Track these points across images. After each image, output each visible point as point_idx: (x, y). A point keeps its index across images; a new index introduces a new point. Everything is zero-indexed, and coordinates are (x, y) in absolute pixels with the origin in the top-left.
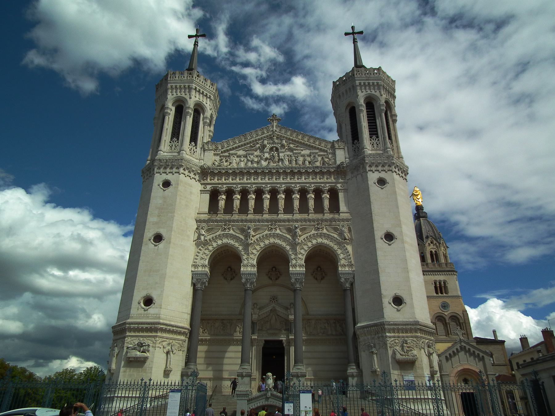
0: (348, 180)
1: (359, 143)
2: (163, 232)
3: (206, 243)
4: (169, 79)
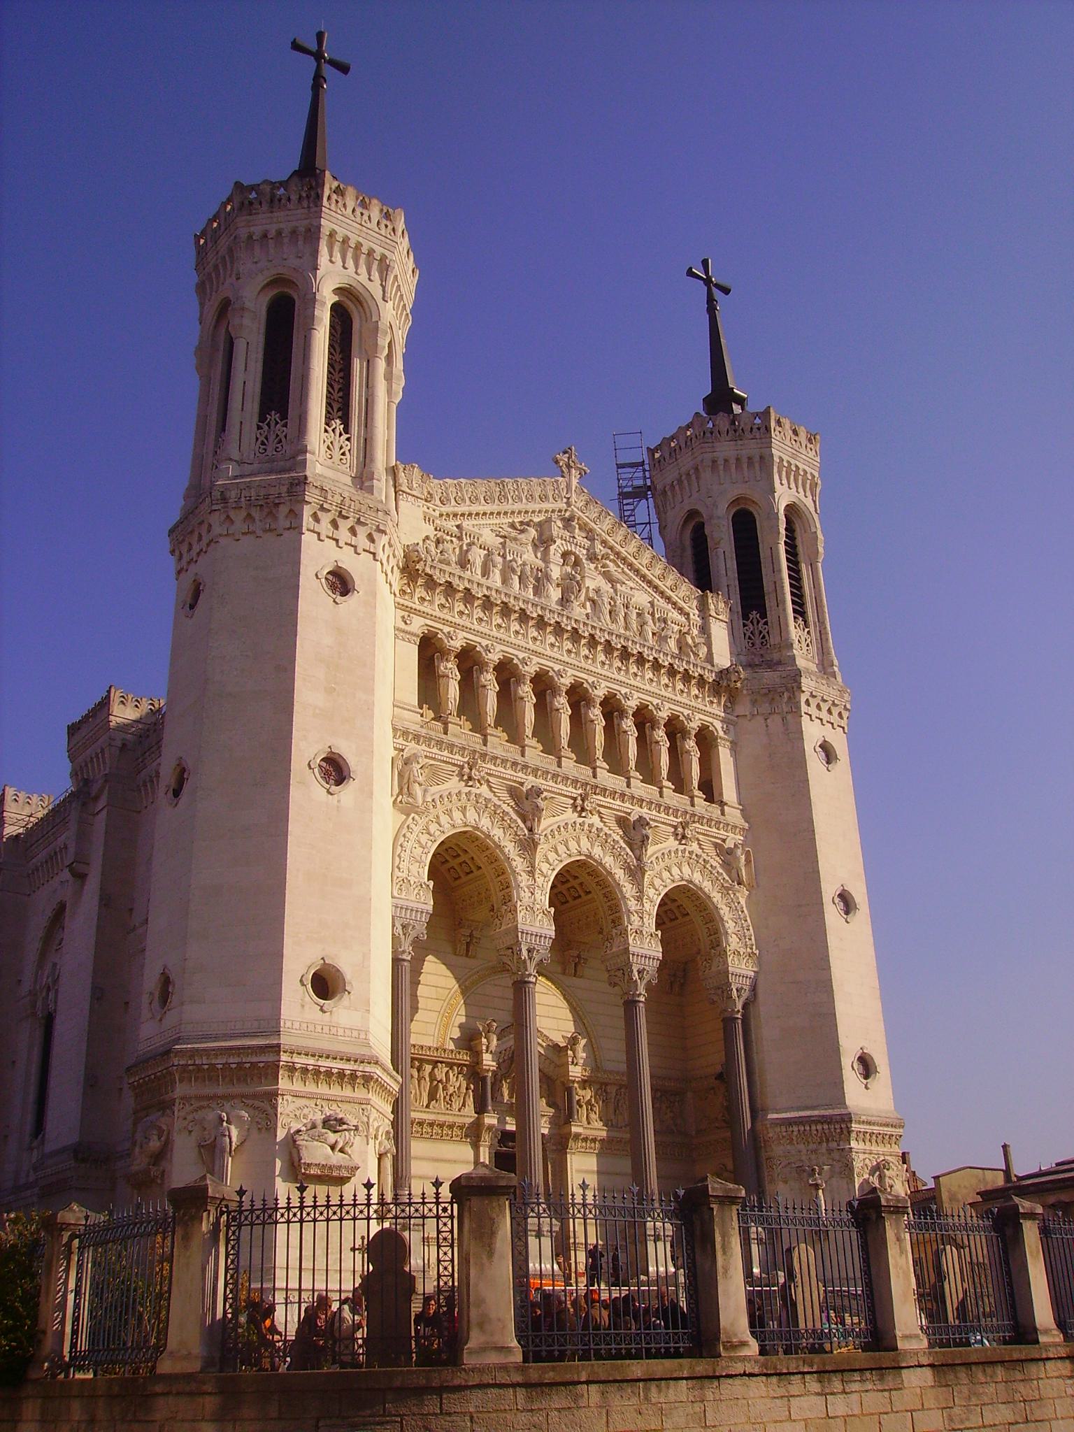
0: (737, 716)
1: (766, 623)
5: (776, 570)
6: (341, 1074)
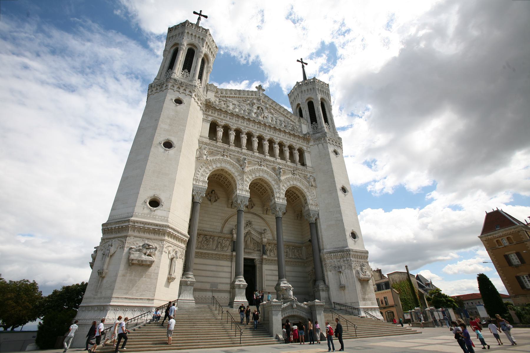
1: (317, 124)
2: (173, 140)
3: (207, 163)
4: (186, 26)
5: (319, 111)
6: (154, 229)
